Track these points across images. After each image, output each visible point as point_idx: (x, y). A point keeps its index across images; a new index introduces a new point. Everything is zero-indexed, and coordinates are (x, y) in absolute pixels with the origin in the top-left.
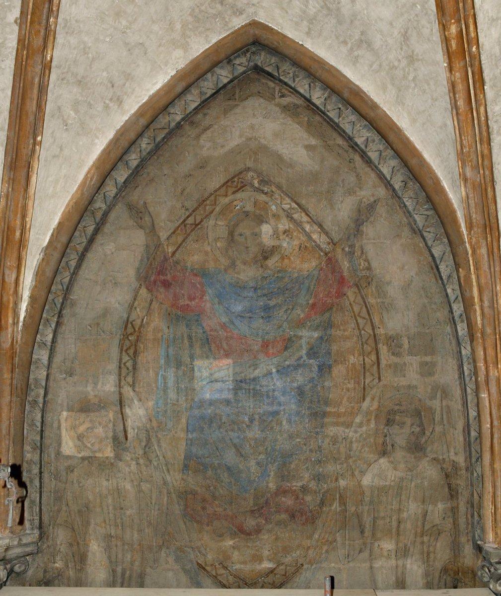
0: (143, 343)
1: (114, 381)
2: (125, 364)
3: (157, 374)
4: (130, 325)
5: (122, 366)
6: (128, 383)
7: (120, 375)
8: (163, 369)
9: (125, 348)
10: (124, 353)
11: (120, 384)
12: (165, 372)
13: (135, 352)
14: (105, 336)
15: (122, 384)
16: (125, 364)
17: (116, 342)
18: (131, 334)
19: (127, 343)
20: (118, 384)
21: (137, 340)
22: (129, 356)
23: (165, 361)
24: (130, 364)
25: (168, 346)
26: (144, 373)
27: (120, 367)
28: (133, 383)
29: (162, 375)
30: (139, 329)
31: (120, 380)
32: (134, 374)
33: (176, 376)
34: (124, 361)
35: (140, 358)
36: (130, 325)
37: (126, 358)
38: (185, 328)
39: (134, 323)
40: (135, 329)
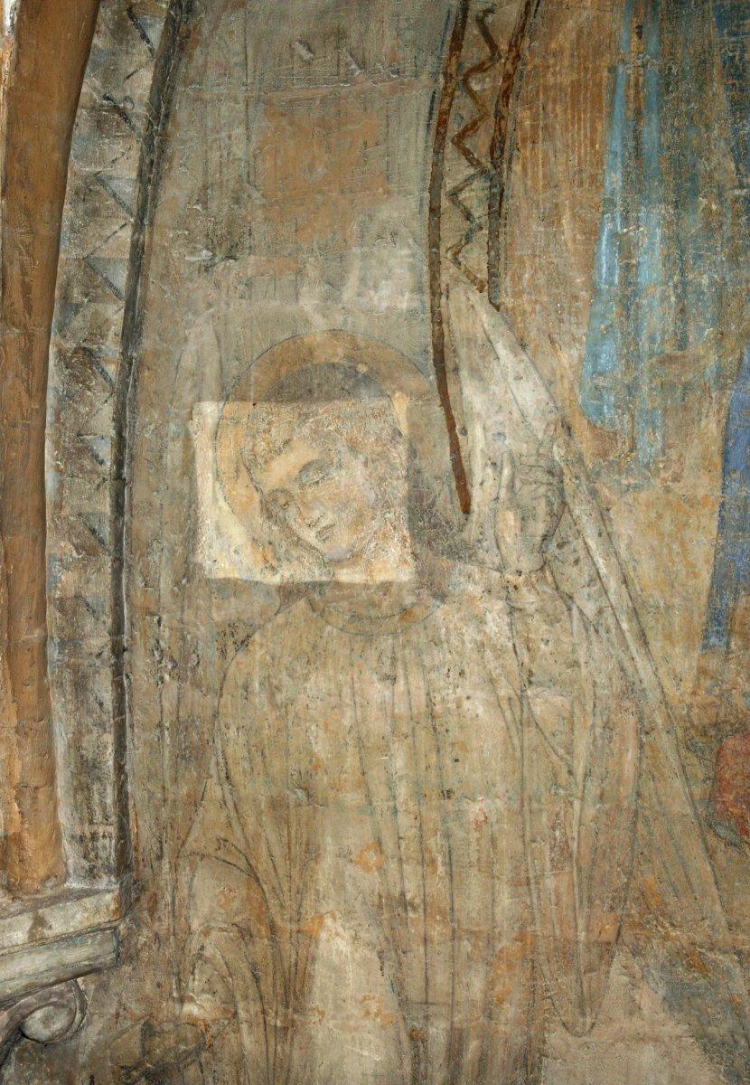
0: (530, 104)
1: (412, 267)
2: (454, 194)
3: (592, 234)
4: (473, 31)
5: (445, 203)
6: (468, 273)
7: (434, 243)
8: (619, 209)
9: (453, 129)
10: (449, 147)
11: (434, 277)
12: (626, 220)
13: (498, 147)
14: (369, 84)
15: (445, 279)
16: (454, 194)
17: (417, 101)
18: (480, 68)
19: (464, 108)
20: (426, 278)
21: (506, 94)
22: (472, 162)
23: (626, 175)
24: (475, 197)
25: (638, 112)
26: (536, 228)
27: (434, 211)
28: (491, 275)
29: (614, 235)
30: (514, 45)
31: (435, 265)
32: (494, 235)
33: (675, 240)
34: (449, 184)
35: (517, 168)
36: (473, 31)
37: (457, 170)
38: (714, 32)
39: (490, 19)
40: (493, 47)
